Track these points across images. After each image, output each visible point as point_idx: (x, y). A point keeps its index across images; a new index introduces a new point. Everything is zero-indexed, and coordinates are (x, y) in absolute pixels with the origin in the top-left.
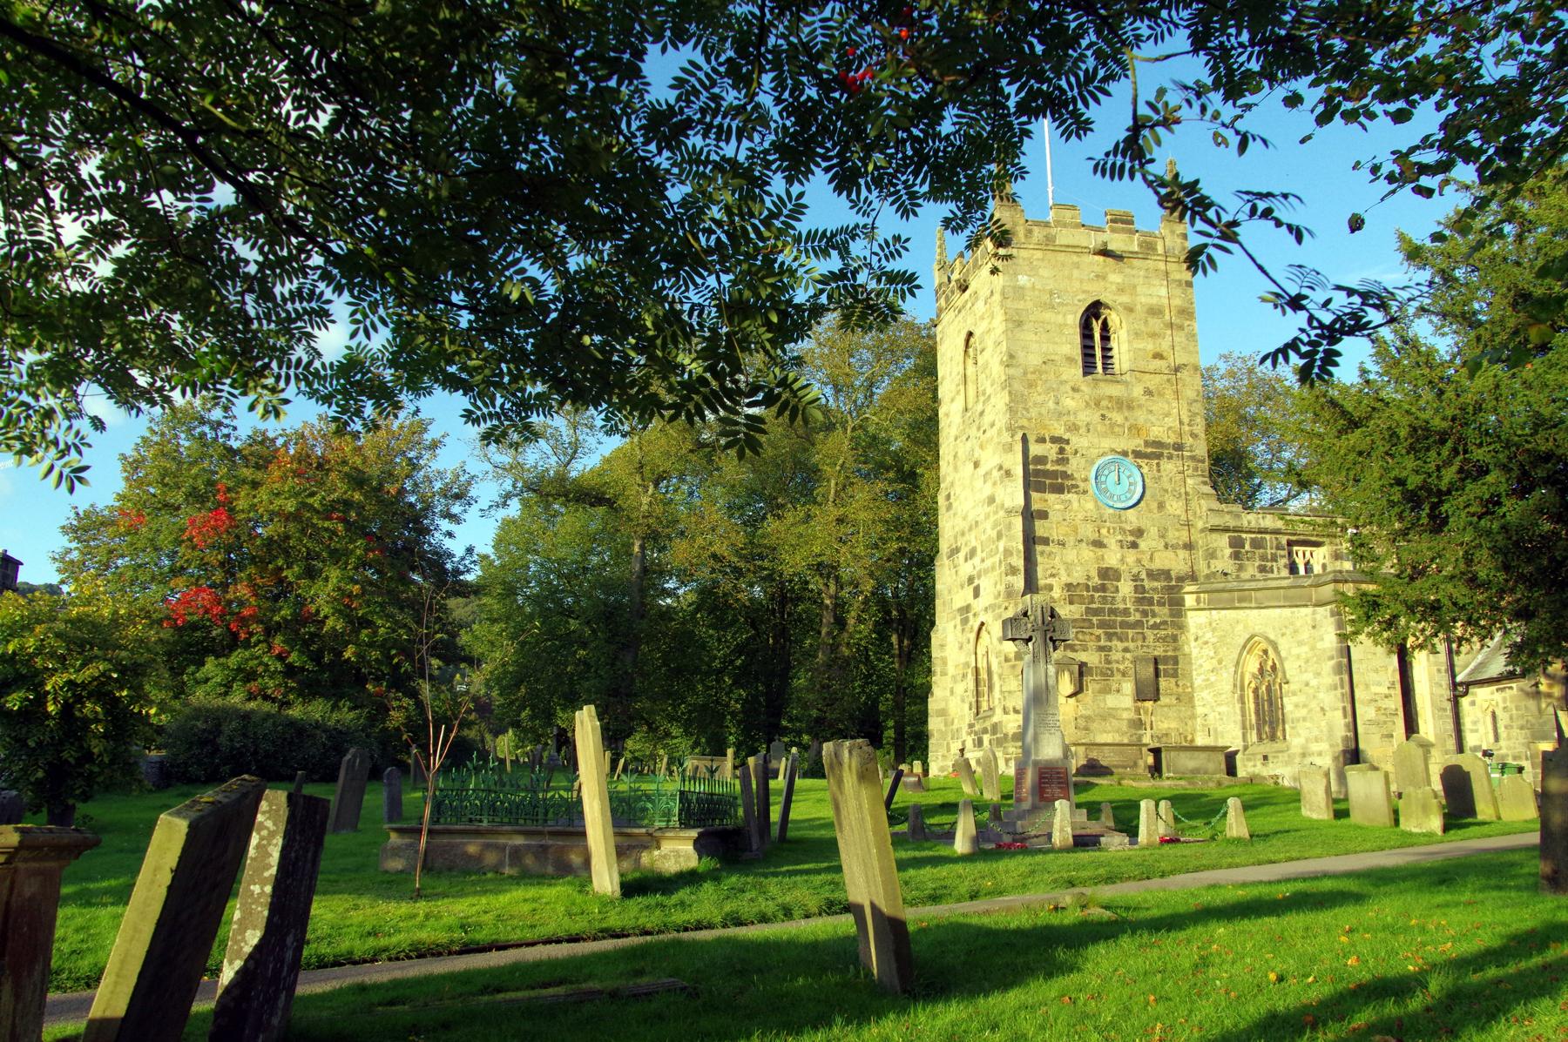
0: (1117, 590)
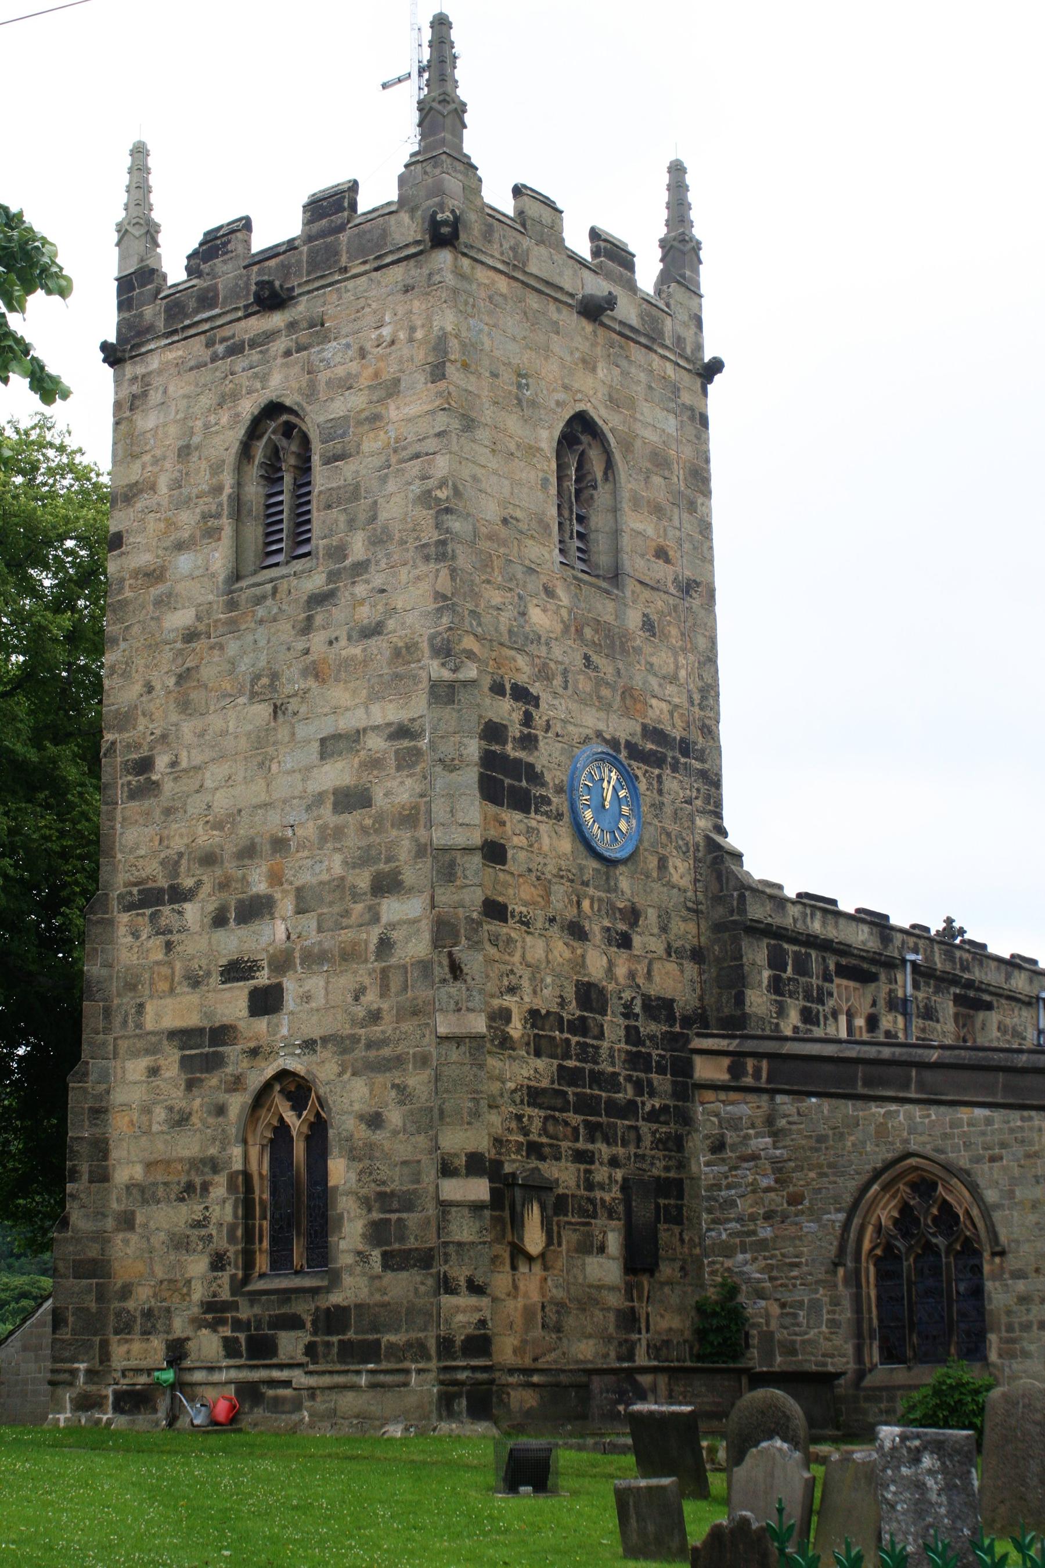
0: (601, 1036)
